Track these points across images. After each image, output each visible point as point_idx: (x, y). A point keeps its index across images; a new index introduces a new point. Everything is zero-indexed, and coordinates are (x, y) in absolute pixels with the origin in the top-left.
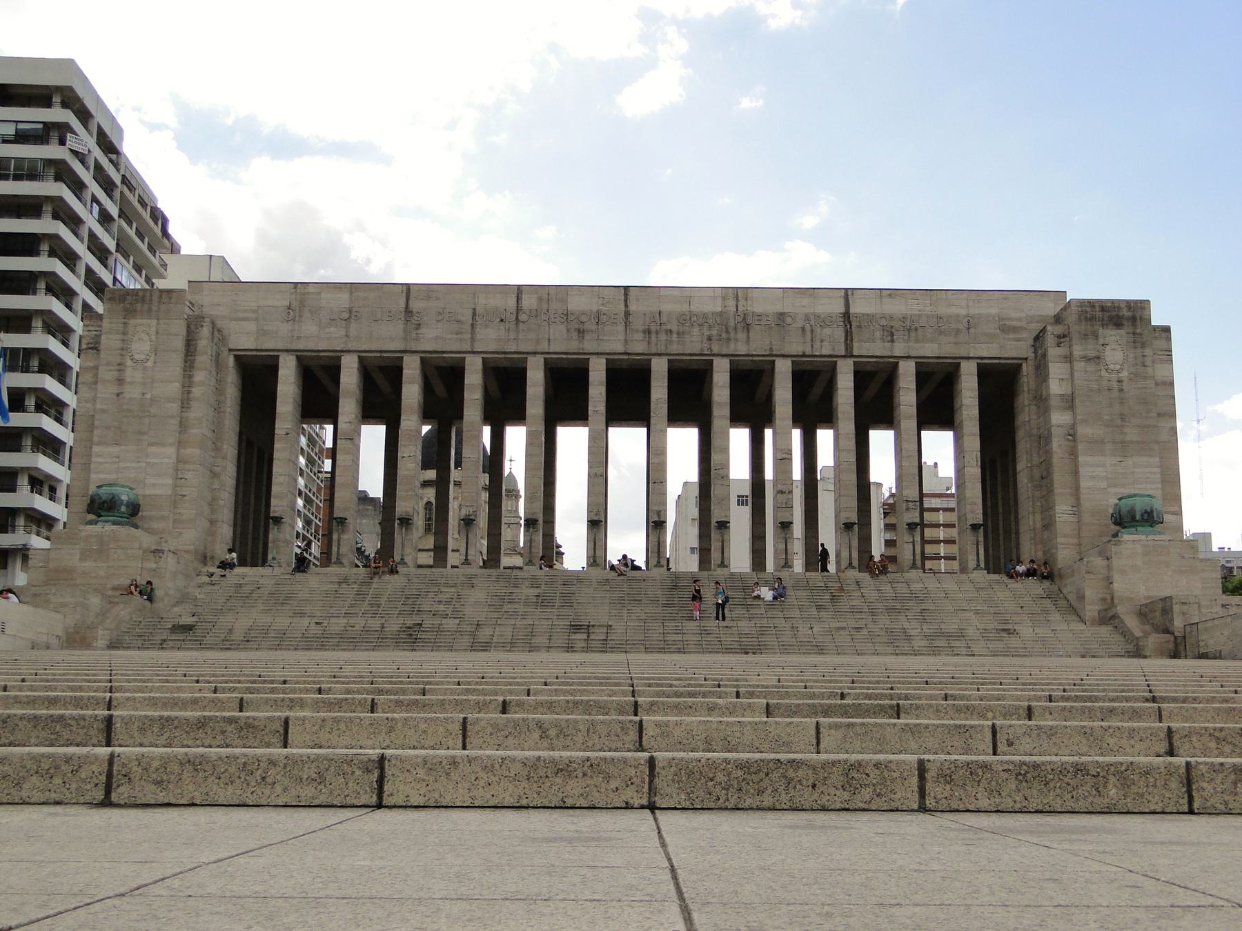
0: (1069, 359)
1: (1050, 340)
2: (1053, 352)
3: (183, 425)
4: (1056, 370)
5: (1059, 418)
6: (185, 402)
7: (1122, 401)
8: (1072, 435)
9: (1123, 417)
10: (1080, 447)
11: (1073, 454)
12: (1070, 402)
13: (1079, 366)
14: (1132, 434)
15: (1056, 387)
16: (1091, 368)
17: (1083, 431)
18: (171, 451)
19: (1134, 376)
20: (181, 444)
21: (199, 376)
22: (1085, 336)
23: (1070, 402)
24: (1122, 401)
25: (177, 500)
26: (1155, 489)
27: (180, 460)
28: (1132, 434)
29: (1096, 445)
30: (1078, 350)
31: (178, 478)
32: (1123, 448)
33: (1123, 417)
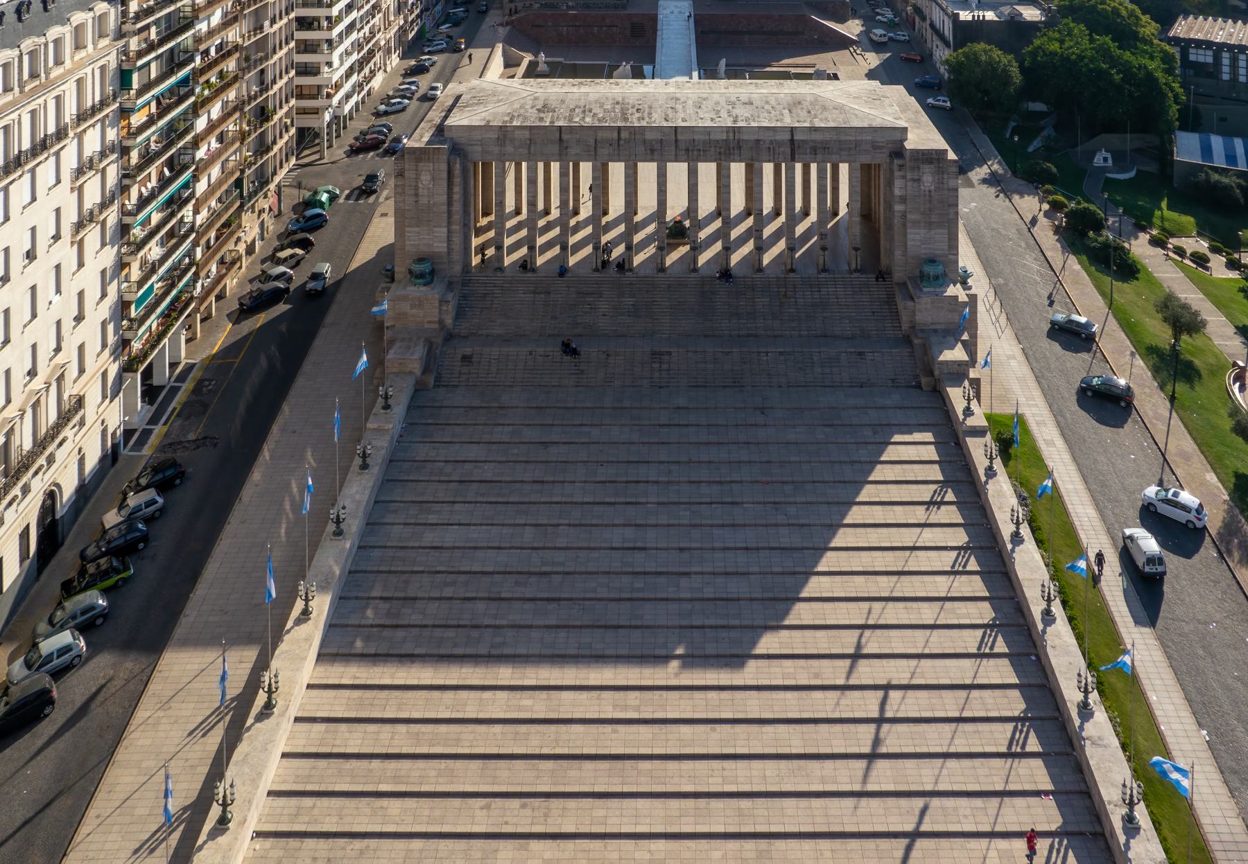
0: (904, 177)
1: (896, 168)
2: (897, 174)
3: (450, 213)
4: (898, 183)
5: (898, 208)
6: (450, 202)
7: (930, 202)
8: (904, 216)
9: (930, 210)
10: (909, 225)
11: (904, 225)
12: (903, 200)
13: (910, 184)
14: (934, 218)
15: (897, 192)
16: (916, 185)
17: (909, 216)
18: (445, 230)
19: (937, 189)
20: (449, 223)
21: (457, 189)
22: (913, 169)
23: (903, 200)
24: (930, 202)
25: (450, 251)
26: (945, 246)
27: (449, 231)
28: (934, 218)
29: (916, 224)
30: (909, 176)
31: (449, 240)
32: (929, 225)
33: (930, 210)
